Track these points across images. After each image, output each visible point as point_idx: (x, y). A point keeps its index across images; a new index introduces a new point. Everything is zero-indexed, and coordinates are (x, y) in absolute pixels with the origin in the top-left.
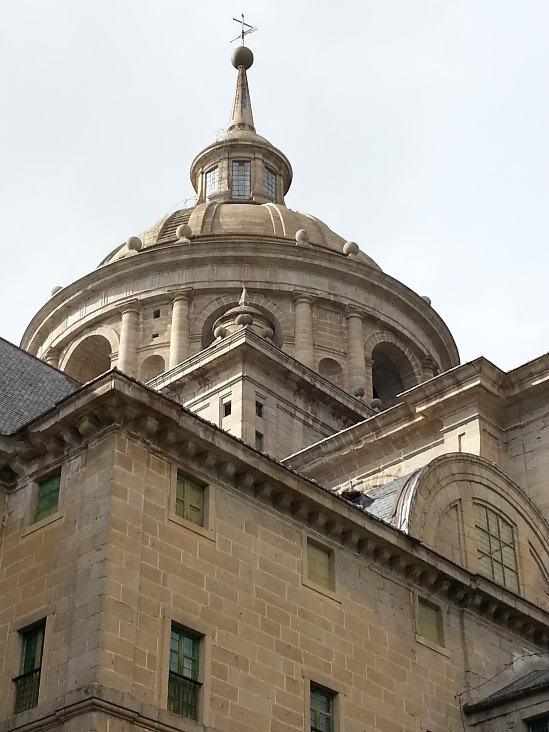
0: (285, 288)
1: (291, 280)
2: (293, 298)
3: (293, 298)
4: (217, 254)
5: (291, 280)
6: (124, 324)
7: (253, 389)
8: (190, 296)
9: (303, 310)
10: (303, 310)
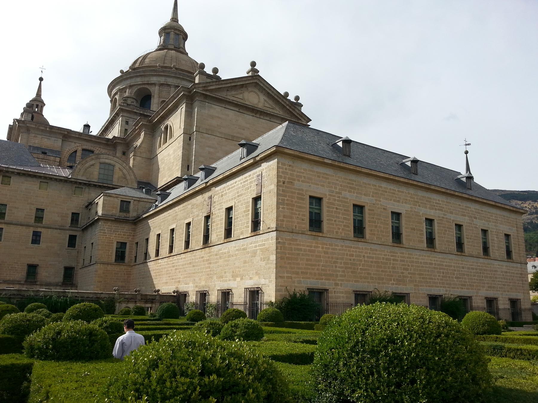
0: (152, 82)
1: (154, 79)
2: (154, 84)
5: (154, 79)
7: (124, 118)
9: (157, 87)
10: (157, 87)
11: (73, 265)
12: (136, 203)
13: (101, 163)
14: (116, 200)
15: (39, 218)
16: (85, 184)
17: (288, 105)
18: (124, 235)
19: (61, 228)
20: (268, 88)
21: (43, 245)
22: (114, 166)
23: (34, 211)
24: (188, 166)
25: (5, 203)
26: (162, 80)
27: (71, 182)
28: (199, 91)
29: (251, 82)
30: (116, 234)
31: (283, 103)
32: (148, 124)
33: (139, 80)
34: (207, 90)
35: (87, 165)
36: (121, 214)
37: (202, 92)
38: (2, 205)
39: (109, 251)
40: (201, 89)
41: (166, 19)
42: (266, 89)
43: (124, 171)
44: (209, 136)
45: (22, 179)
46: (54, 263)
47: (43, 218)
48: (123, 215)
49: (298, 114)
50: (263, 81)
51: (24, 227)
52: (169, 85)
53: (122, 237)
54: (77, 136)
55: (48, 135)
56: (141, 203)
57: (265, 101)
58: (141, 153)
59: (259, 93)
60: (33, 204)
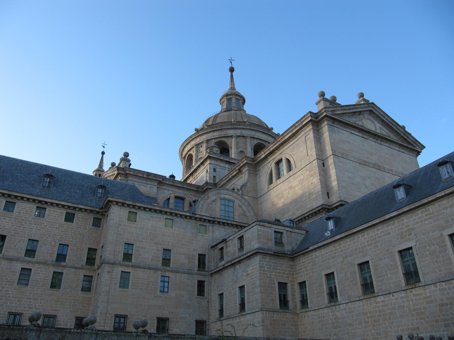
0: (229, 135)
1: (231, 132)
2: (231, 137)
3: (231, 137)
4: (212, 130)
5: (231, 132)
6: (194, 149)
8: (208, 141)
10: (234, 140)
11: (204, 318)
12: (289, 233)
13: (221, 199)
14: (269, 230)
15: (166, 262)
16: (209, 221)
17: (402, 132)
18: (284, 273)
19: (189, 273)
20: (382, 116)
21: (172, 293)
22: (233, 202)
23: (161, 252)
24: (328, 193)
25: (131, 242)
26: (238, 132)
27: (196, 218)
28: (329, 115)
29: (367, 109)
30: (276, 272)
31: (397, 130)
32: (251, 163)
33: (216, 134)
34: (335, 114)
35: (209, 201)
36: (277, 247)
37: (331, 116)
38: (129, 244)
39: (272, 294)
40: (330, 113)
41: (225, 88)
42: (381, 116)
43: (244, 207)
44: (345, 160)
45: (148, 215)
46: (184, 316)
47: (170, 260)
48: (279, 249)
49: (412, 141)
50: (377, 109)
51: (152, 271)
52: (244, 137)
53: (282, 276)
54: (171, 183)
55: (145, 182)
56: (293, 235)
57: (380, 128)
58: (247, 192)
59: (374, 121)
60: (160, 244)
